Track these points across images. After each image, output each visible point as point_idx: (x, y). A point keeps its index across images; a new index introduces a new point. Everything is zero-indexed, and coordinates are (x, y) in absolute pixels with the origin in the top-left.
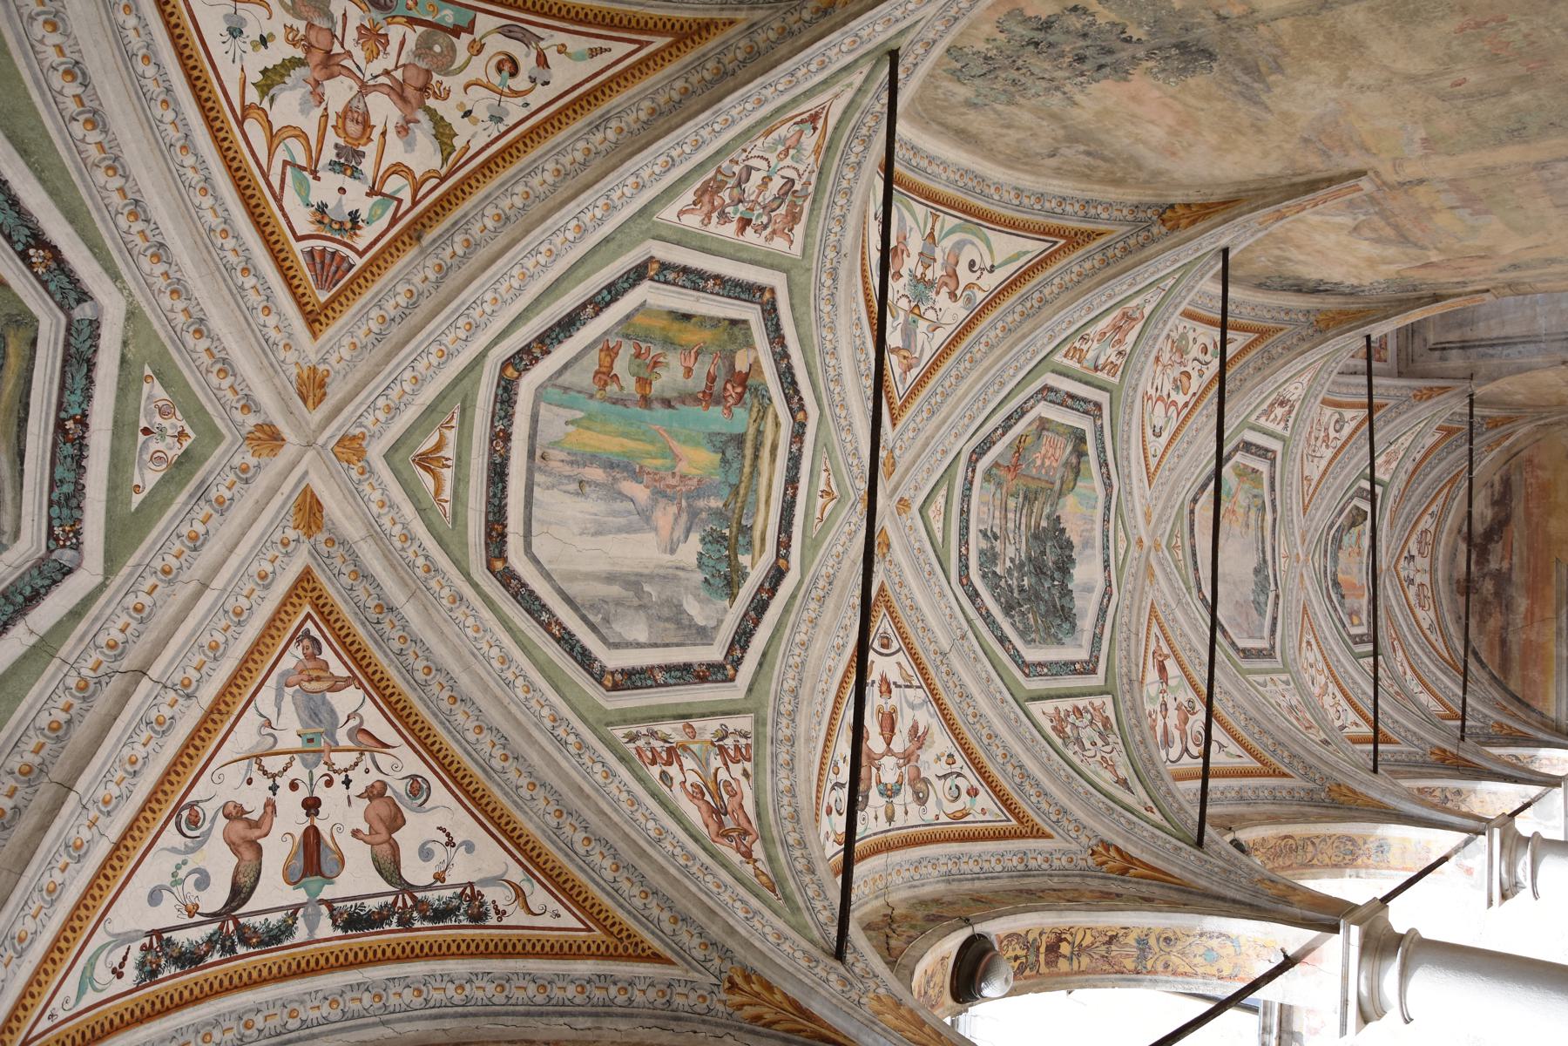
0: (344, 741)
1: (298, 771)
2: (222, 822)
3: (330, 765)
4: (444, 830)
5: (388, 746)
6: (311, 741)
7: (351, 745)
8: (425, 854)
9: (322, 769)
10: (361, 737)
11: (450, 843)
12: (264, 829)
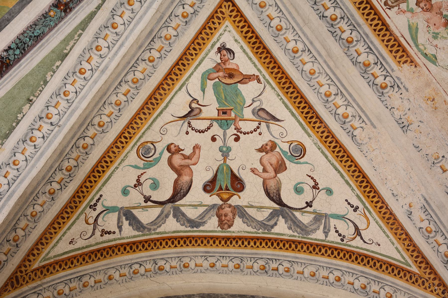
0: (248, 113)
1: (216, 130)
2: (167, 155)
3: (238, 129)
4: (312, 178)
5: (278, 120)
6: (224, 113)
7: (252, 117)
8: (298, 190)
9: (232, 131)
10: (261, 113)
11: (315, 187)
12: (194, 160)
